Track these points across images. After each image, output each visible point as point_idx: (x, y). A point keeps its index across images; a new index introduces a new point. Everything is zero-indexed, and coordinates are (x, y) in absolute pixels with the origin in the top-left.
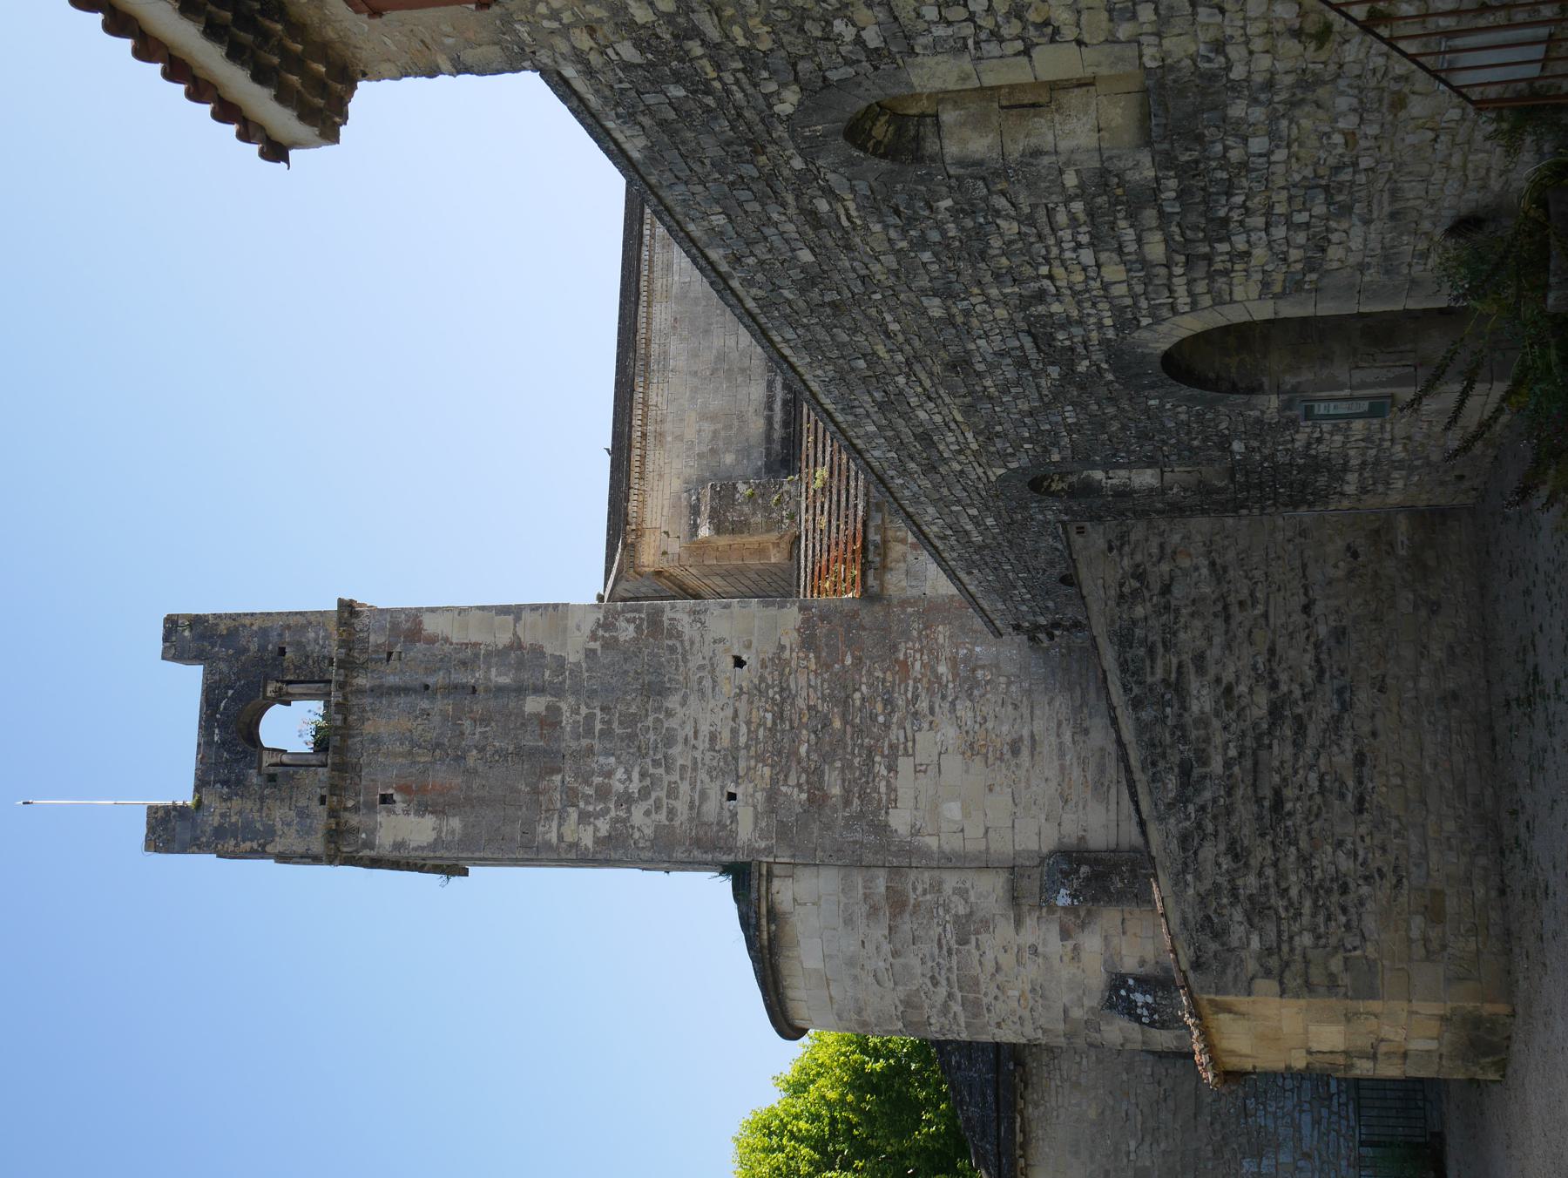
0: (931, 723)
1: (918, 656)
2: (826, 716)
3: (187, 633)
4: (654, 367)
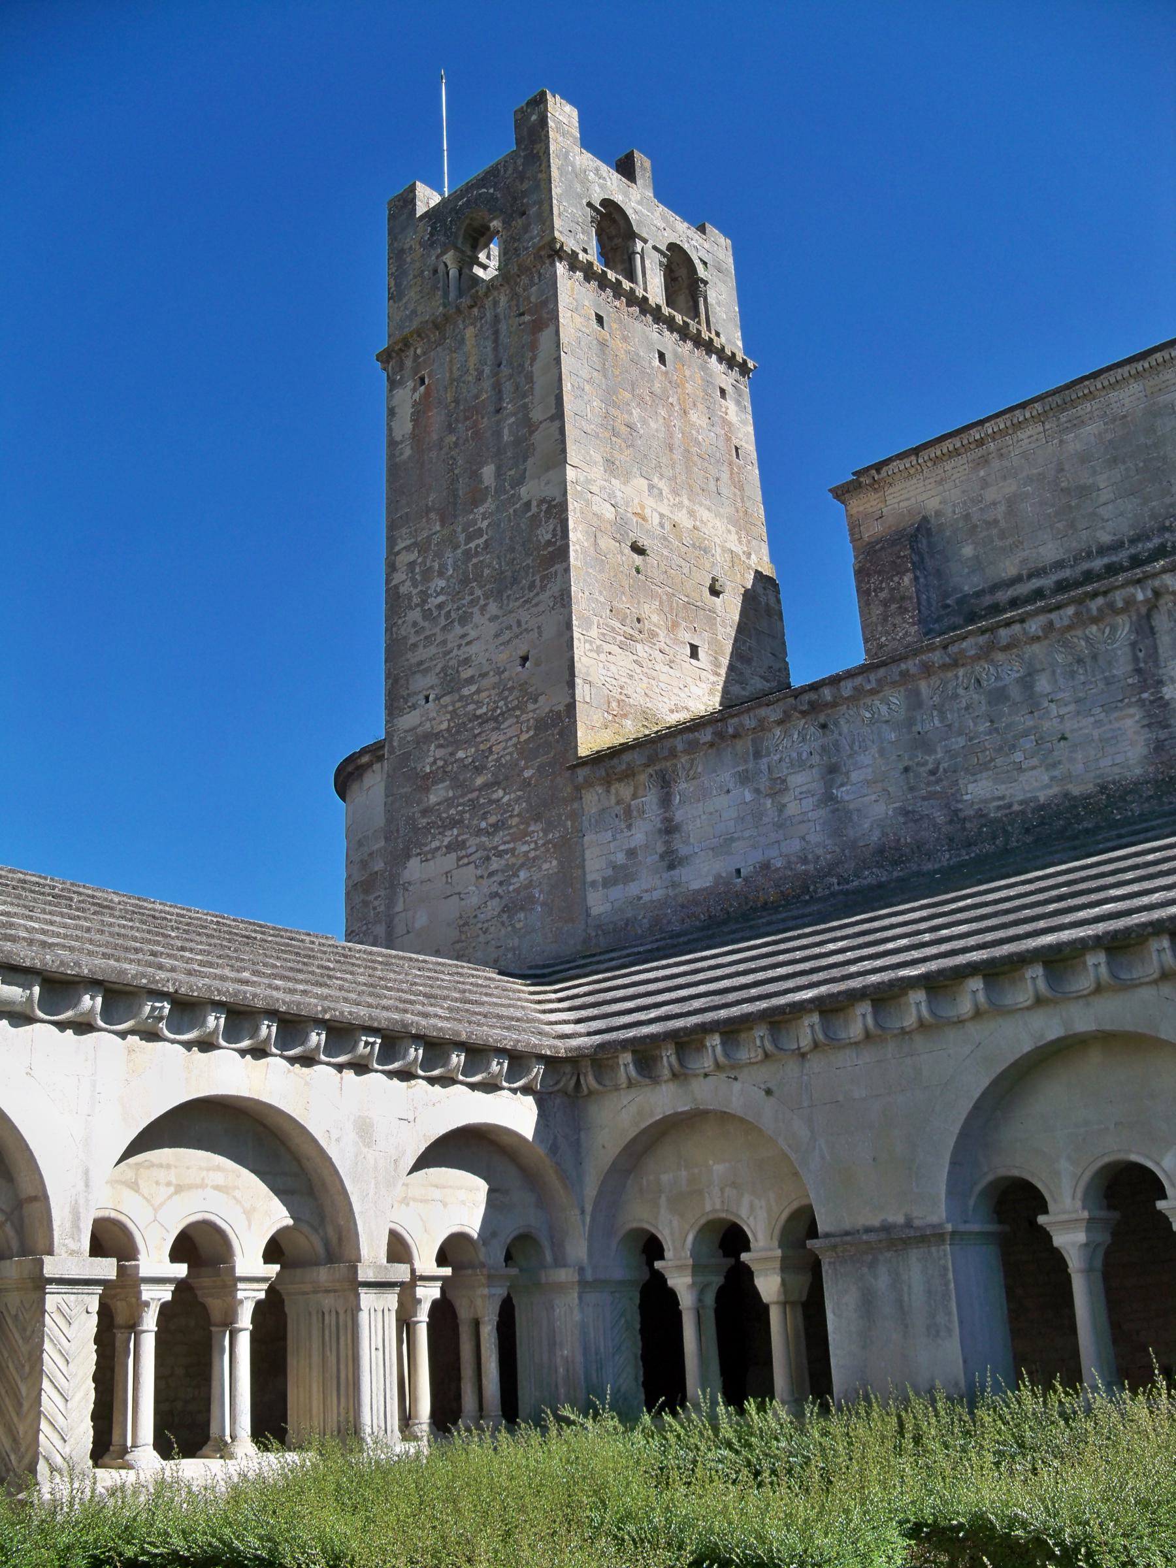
0: (482, 877)
1: (532, 846)
2: (484, 767)
3: (534, 118)
4: (1063, 418)
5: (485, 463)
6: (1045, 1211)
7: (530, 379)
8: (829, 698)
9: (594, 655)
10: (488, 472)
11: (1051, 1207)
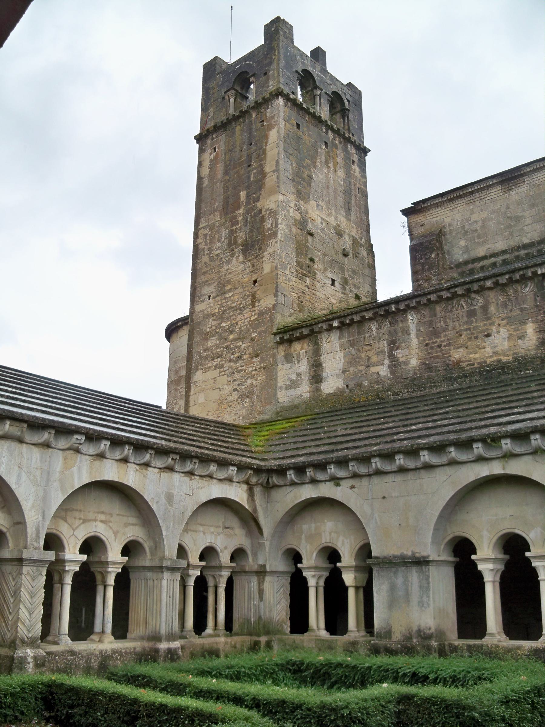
0: (230, 381)
1: (254, 368)
2: (234, 331)
3: (273, 29)
5: (243, 190)
6: (475, 553)
7: (264, 152)
8: (394, 309)
9: (287, 282)
10: (243, 195)
11: (478, 552)
